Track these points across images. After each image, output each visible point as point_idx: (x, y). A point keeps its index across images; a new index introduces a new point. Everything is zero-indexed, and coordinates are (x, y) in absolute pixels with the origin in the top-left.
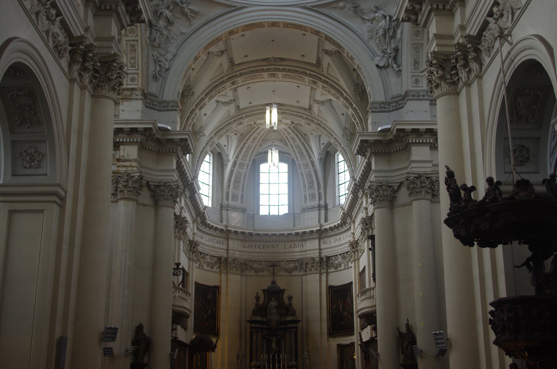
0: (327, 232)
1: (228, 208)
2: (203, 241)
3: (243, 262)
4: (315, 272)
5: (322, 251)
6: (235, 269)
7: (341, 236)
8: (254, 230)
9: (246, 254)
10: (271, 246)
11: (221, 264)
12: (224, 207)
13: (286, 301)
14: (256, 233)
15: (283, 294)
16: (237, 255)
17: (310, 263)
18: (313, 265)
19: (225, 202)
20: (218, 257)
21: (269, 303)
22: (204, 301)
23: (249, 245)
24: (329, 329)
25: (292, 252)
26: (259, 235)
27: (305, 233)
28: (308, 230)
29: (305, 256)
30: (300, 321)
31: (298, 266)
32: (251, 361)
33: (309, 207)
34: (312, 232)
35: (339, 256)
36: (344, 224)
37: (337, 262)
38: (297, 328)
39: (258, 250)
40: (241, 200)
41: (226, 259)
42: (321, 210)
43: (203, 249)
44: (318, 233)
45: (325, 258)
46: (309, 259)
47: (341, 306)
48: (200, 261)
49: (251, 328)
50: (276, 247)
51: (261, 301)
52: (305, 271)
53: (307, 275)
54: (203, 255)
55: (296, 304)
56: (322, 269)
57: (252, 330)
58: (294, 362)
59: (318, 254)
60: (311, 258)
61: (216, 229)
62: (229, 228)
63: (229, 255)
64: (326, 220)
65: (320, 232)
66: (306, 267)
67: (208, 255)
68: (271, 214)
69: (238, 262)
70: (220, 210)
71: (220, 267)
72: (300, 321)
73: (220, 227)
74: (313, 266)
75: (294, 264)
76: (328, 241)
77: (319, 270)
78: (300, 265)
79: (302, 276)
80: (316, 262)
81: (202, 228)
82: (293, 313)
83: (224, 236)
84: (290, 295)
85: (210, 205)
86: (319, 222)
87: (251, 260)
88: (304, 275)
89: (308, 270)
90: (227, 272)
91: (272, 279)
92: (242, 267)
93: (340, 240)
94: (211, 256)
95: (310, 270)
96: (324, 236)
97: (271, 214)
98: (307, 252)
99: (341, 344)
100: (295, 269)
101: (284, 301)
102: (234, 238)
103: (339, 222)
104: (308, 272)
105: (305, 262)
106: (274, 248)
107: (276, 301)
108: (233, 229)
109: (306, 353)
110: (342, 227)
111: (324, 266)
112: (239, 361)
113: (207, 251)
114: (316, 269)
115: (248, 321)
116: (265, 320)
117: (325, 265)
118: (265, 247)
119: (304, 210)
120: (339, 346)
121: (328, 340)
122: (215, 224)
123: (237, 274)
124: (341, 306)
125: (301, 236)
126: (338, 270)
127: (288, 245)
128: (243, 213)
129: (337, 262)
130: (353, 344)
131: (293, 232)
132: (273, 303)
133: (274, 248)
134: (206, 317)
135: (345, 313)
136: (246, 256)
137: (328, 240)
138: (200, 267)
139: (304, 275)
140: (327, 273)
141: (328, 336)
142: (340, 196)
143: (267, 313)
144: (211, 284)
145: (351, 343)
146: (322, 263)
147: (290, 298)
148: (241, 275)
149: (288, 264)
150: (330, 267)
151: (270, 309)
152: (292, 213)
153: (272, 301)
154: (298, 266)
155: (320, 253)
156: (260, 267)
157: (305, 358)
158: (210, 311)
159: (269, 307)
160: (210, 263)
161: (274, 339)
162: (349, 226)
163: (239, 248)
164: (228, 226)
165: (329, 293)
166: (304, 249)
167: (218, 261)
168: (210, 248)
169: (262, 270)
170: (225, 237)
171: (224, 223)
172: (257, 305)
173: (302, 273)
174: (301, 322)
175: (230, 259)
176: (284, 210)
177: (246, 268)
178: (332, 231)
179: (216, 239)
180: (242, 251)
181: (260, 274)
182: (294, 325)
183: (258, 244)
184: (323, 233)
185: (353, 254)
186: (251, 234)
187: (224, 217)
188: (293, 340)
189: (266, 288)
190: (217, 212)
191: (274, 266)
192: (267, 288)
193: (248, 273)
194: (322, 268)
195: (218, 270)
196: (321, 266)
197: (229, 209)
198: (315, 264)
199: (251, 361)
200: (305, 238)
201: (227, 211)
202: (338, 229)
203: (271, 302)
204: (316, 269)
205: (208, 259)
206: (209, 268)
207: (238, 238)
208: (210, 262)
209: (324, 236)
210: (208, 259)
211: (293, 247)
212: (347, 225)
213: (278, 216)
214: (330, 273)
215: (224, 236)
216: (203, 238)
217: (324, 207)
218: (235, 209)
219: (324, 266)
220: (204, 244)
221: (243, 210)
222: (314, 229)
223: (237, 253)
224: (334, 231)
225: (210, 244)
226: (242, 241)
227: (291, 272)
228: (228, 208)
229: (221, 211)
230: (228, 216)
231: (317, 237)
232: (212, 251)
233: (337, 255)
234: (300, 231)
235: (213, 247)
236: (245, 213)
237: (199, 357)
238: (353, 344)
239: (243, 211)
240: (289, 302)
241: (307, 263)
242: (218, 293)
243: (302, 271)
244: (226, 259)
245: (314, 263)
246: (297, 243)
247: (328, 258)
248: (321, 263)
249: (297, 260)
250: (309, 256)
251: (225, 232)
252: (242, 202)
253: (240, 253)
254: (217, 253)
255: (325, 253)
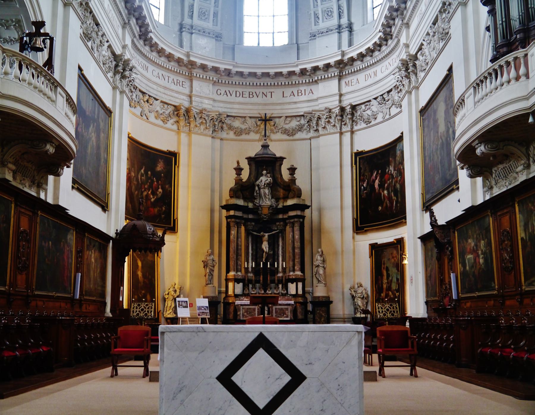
0: (352, 65)
1: (192, 30)
2: (149, 75)
3: (216, 117)
4: (332, 131)
5: (343, 98)
6: (202, 127)
7: (378, 68)
8: (234, 66)
9: (222, 105)
10: (261, 93)
11: (179, 117)
12: (185, 28)
13: (286, 175)
14: (237, 72)
15: (281, 164)
16: (207, 104)
17: (325, 117)
18: (330, 120)
19: (187, 21)
20: (175, 106)
21: (257, 179)
22: (149, 173)
23: (226, 91)
24: (355, 221)
25: (295, 103)
26: (241, 74)
27: (316, 69)
28: (321, 64)
29: (317, 108)
30: (307, 207)
31: (304, 125)
32: (228, 271)
33: (323, 31)
34: (328, 66)
35: (374, 102)
36: (385, 43)
37: (369, 112)
38: (303, 217)
39: (240, 99)
40: (213, 20)
41: (188, 111)
42: (342, 32)
43: (148, 88)
44: (337, 68)
45: (349, 107)
46: (323, 111)
47: (377, 182)
48: (141, 107)
49: (227, 217)
50: (269, 95)
51: (245, 175)
52: (315, 131)
53: (318, 137)
54: (147, 97)
55: (301, 182)
56: (343, 126)
57: (229, 220)
58: (299, 273)
59: (337, 103)
60: (326, 108)
61: (170, 57)
62: (192, 59)
63: (194, 103)
64: (350, 44)
65: (341, 66)
66: (317, 124)
67: (157, 100)
68: (261, 45)
69: (208, 116)
70: (178, 33)
71: (177, 122)
72: (307, 207)
73: (177, 55)
74: (329, 122)
75: (298, 121)
76: (355, 81)
77: (339, 128)
78: (308, 122)
79: (310, 139)
80: (335, 115)
81: (146, 50)
82: (298, 194)
83: (184, 73)
84: (293, 165)
85: (162, 21)
86: (340, 47)
87: (229, 114)
88: (314, 138)
89: (320, 129)
90: (190, 130)
91: (261, 143)
92: (215, 125)
93: (375, 74)
94: (162, 102)
95: (324, 128)
96: (347, 73)
97: (261, 45)
98: (320, 101)
99: (377, 243)
100: (300, 128)
101: (281, 175)
102: (201, 76)
103: (376, 39)
104: (321, 131)
105: (316, 116)
106: (266, 96)
107: (269, 175)
108: (199, 62)
109: (319, 258)
110: (379, 50)
111: (348, 121)
112: (208, 271)
113: (155, 92)
114: (334, 126)
115: (223, 207)
116: (251, 205)
117: (349, 119)
118: (251, 96)
119: (313, 36)
120: (374, 247)
121: (353, 238)
122: (169, 46)
123: (206, 135)
124: (377, 182)
125: (310, 75)
126: (371, 124)
127: (288, 91)
128: (216, 40)
129: (369, 112)
130: (400, 243)
131: (297, 70)
132: (265, 179)
133: (266, 96)
134: (153, 200)
135: (386, 192)
136: (221, 107)
137: (353, 78)
138: (142, 116)
139: (314, 138)
140: (352, 132)
141: (354, 232)
142: (373, 8)
143: (255, 194)
144: (164, 147)
145: (396, 239)
146: (344, 117)
147: (292, 170)
148: (213, 137)
149: (287, 122)
150: (357, 123)
151: (259, 189)
152: (295, 42)
153: (262, 175)
154: (304, 125)
155: (340, 101)
156: (243, 127)
157: (318, 266)
158: (160, 190)
159: (258, 185)
160: (161, 114)
161: (267, 235)
162: (396, 40)
163: (209, 94)
164: (190, 53)
165: (356, 164)
166: (315, 97)
167: (176, 113)
168: (162, 90)
169: (248, 132)
170: (187, 74)
171: (186, 49)
172: (238, 181)
173: (312, 134)
174: (310, 208)
175: (195, 110)
176: (282, 40)
177: (222, 128)
178: (362, 61)
179: (172, 76)
180: (214, 100)
181: (244, 137)
182: (299, 213)
183: (240, 90)
184: (346, 68)
185: (406, 82)
186: (228, 73)
187: (185, 43)
188: (297, 237)
189: (253, 155)
190: (174, 35)
191: (265, 120)
192: (255, 156)
193: (224, 135)
194: (345, 124)
195: (175, 127)
196: (342, 121)
197: (194, 31)
198: (333, 118)
199: (228, 271)
200: (316, 78)
201: (189, 35)
202: (371, 56)
203: (261, 178)
204: (334, 126)
205: (157, 106)
206: (159, 122)
207: (208, 78)
208: (161, 112)
209: (347, 73)
210: (157, 106)
211: (296, 94)
212: (390, 42)
213: (273, 49)
214: (357, 132)
215: (184, 73)
216: (147, 69)
217: (346, 27)
218: (204, 32)
219: (348, 121)
220: (149, 80)
221: (217, 37)
222: (332, 61)
223: (207, 102)
224: (364, 61)
225: (161, 82)
226: (214, 83)
227: (293, 135)
228: (192, 30)
229: (181, 35)
230: (191, 43)
231: (336, 74)
232: (164, 94)
233: (370, 101)
234: (309, 66)
235: (165, 88)
236: (221, 41)
237: (140, 264)
238: (400, 243)
239: (218, 37)
240: (290, 176)
241: (319, 118)
242: (175, 164)
243: (311, 131)
244: (188, 111)
245: (330, 117)
246: (302, 88)
247: (354, 108)
248: (342, 116)
249: (303, 116)
250: (322, 107)
251: (186, 66)
252: (215, 23)
253: (211, 102)
254: (172, 98)
255: (347, 102)
